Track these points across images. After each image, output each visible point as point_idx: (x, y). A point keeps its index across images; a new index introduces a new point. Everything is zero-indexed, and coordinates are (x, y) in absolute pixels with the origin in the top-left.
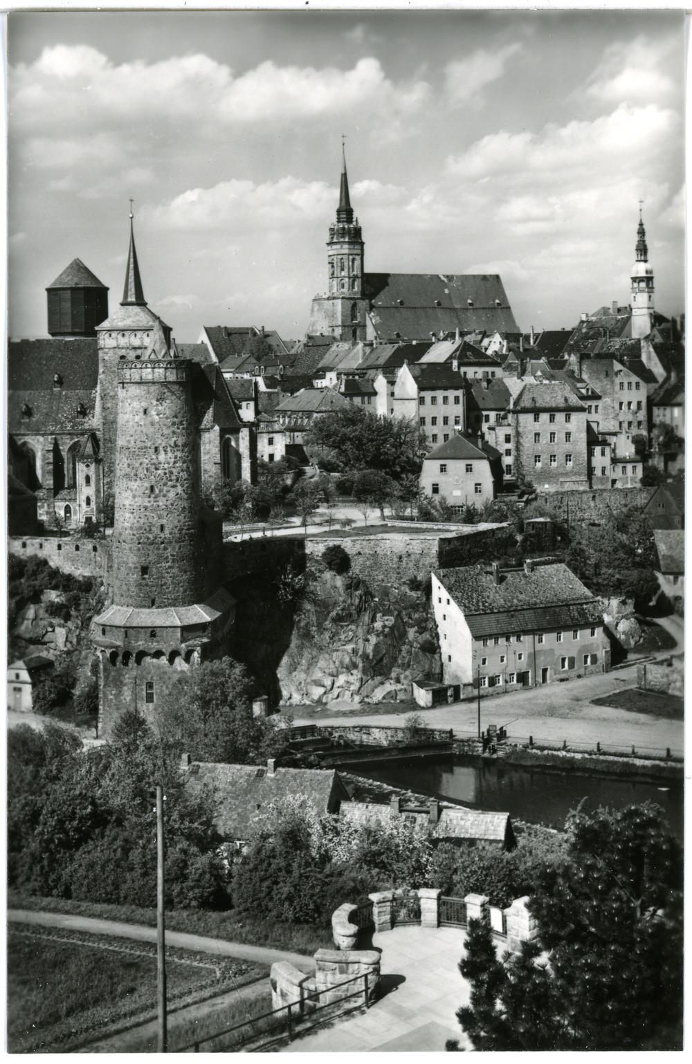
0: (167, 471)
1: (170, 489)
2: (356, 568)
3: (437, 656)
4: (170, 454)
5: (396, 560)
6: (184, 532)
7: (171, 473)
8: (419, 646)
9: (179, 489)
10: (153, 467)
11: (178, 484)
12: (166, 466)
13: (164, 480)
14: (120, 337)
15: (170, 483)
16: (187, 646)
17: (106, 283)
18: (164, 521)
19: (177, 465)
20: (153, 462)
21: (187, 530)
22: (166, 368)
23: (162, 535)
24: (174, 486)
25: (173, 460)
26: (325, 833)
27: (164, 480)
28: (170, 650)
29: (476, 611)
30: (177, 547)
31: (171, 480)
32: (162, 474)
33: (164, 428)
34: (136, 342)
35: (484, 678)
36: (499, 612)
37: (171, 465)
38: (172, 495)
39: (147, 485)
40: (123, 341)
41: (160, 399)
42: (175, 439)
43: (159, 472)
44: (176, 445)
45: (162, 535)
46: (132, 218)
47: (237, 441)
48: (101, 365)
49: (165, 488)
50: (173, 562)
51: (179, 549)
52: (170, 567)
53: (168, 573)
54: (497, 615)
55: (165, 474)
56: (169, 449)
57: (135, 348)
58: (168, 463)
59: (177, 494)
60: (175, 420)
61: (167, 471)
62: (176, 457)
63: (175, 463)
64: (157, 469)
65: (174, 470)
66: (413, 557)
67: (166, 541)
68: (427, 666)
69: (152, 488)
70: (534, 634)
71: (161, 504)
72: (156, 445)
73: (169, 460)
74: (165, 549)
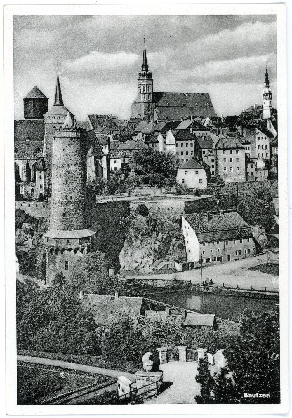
2: (150, 214)
3: (184, 250)
4: (74, 167)
6: (80, 199)
7: (75, 175)
8: (177, 246)
9: (78, 182)
10: (67, 172)
11: (77, 180)
12: (72, 172)
13: (72, 178)
15: (74, 179)
17: (47, 97)
19: (77, 172)
20: (67, 170)
21: (81, 198)
22: (72, 132)
23: (71, 201)
24: (76, 180)
25: (75, 170)
26: (139, 323)
29: (200, 231)
30: (77, 205)
31: (74, 178)
33: (72, 156)
35: (204, 259)
36: (210, 232)
38: (75, 184)
40: (55, 121)
42: (76, 161)
44: (76, 164)
45: (71, 201)
46: (58, 69)
47: (101, 162)
49: (72, 181)
50: (76, 211)
51: (78, 206)
52: (75, 214)
53: (74, 216)
54: (209, 233)
55: (72, 175)
56: (73, 165)
57: (59, 124)
58: (73, 171)
60: (76, 153)
61: (73, 174)
62: (76, 169)
63: (76, 171)
65: (76, 174)
66: (174, 209)
68: (180, 255)
69: (67, 181)
70: (224, 241)
71: (70, 188)
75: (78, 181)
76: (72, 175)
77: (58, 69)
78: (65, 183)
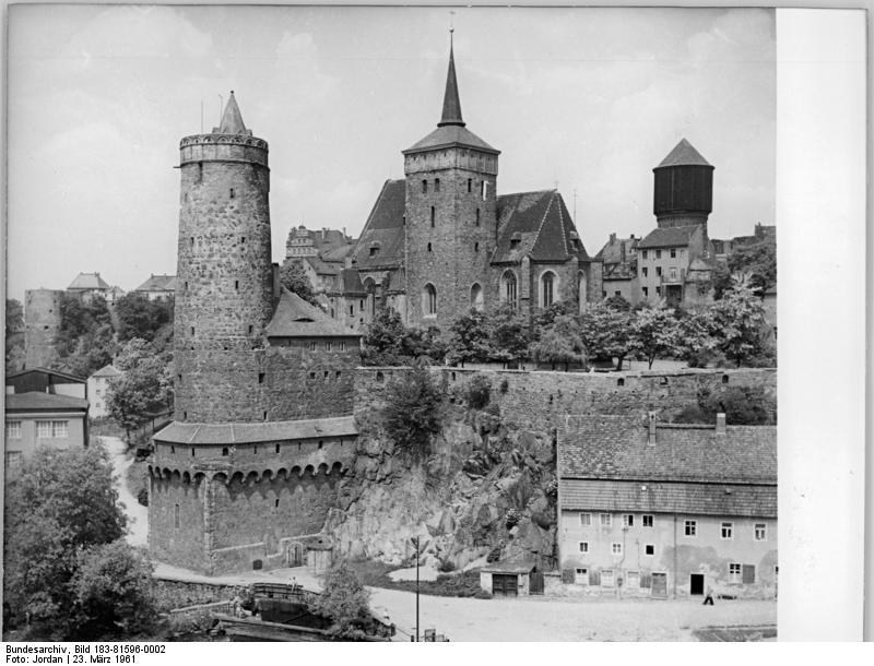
0: (200, 266)
1: (201, 286)
4: (205, 246)
5: (547, 400)
7: (205, 268)
12: (200, 259)
14: (422, 159)
15: (203, 280)
18: (194, 324)
19: (214, 258)
25: (208, 252)
27: (197, 276)
29: (584, 473)
31: (203, 276)
37: (206, 258)
39: (183, 281)
42: (212, 228)
43: (192, 266)
46: (452, 31)
48: (407, 192)
49: (197, 286)
50: (202, 371)
52: (199, 377)
54: (616, 484)
55: (198, 268)
57: (434, 171)
60: (213, 205)
61: (200, 266)
62: (211, 250)
63: (210, 256)
74: (194, 355)
75: (213, 284)
77: (452, 31)
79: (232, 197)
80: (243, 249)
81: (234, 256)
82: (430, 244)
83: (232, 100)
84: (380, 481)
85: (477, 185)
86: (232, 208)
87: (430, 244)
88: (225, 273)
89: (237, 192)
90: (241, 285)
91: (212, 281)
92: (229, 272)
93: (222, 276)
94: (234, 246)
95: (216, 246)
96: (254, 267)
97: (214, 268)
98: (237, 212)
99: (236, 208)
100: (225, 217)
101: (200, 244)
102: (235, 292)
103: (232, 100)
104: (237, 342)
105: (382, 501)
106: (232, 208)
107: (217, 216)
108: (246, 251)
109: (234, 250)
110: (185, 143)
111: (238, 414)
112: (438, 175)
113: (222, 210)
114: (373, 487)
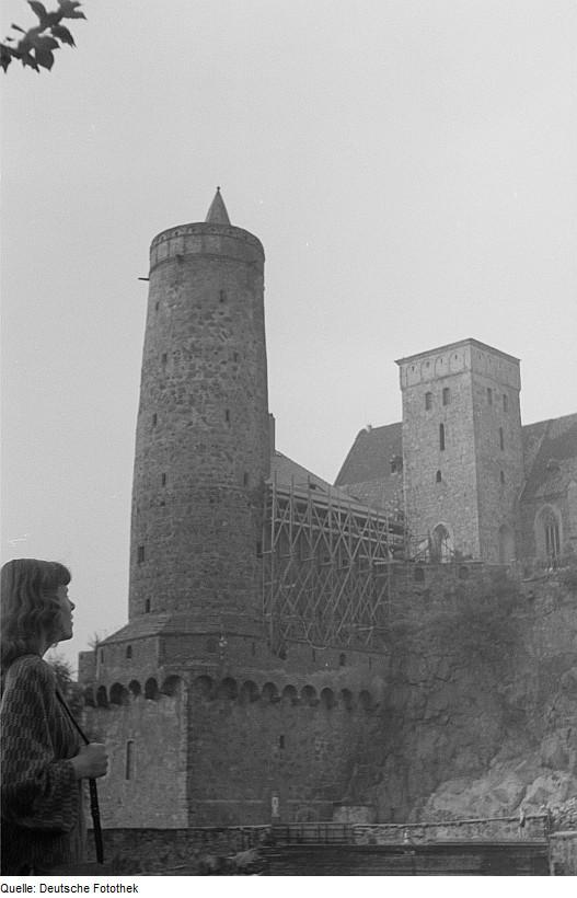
0: (176, 389)
1: (178, 415)
4: (182, 363)
12: (175, 381)
16: (166, 670)
19: (195, 379)
20: (159, 377)
21: (206, 482)
22: (184, 236)
24: (184, 412)
28: (146, 679)
30: (185, 508)
31: (181, 402)
32: (169, 394)
34: (442, 370)
37: (184, 378)
41: (176, 283)
42: (194, 339)
43: (164, 391)
51: (189, 512)
55: (173, 393)
59: (190, 424)
60: (196, 310)
61: (176, 389)
62: (192, 367)
63: (191, 375)
64: (162, 387)
67: (168, 500)
69: (155, 416)
71: (163, 440)
72: (165, 352)
73: (180, 371)
76: (173, 393)
78: (150, 425)
79: (222, 301)
80: (235, 369)
81: (224, 376)
82: (439, 473)
83: (218, 194)
84: (434, 718)
85: (498, 398)
86: (222, 314)
87: (439, 473)
88: (211, 397)
89: (229, 295)
90: (233, 416)
91: (193, 409)
92: (217, 396)
93: (207, 402)
94: (224, 363)
95: (199, 362)
96: (250, 395)
97: (196, 391)
98: (227, 319)
99: (227, 315)
100: (212, 325)
101: (177, 360)
102: (225, 425)
103: (218, 194)
104: (228, 493)
105: (436, 749)
106: (222, 314)
107: (201, 323)
108: (238, 372)
109: (224, 368)
110: (158, 240)
111: (226, 597)
112: (446, 383)
113: (208, 317)
114: (419, 729)
